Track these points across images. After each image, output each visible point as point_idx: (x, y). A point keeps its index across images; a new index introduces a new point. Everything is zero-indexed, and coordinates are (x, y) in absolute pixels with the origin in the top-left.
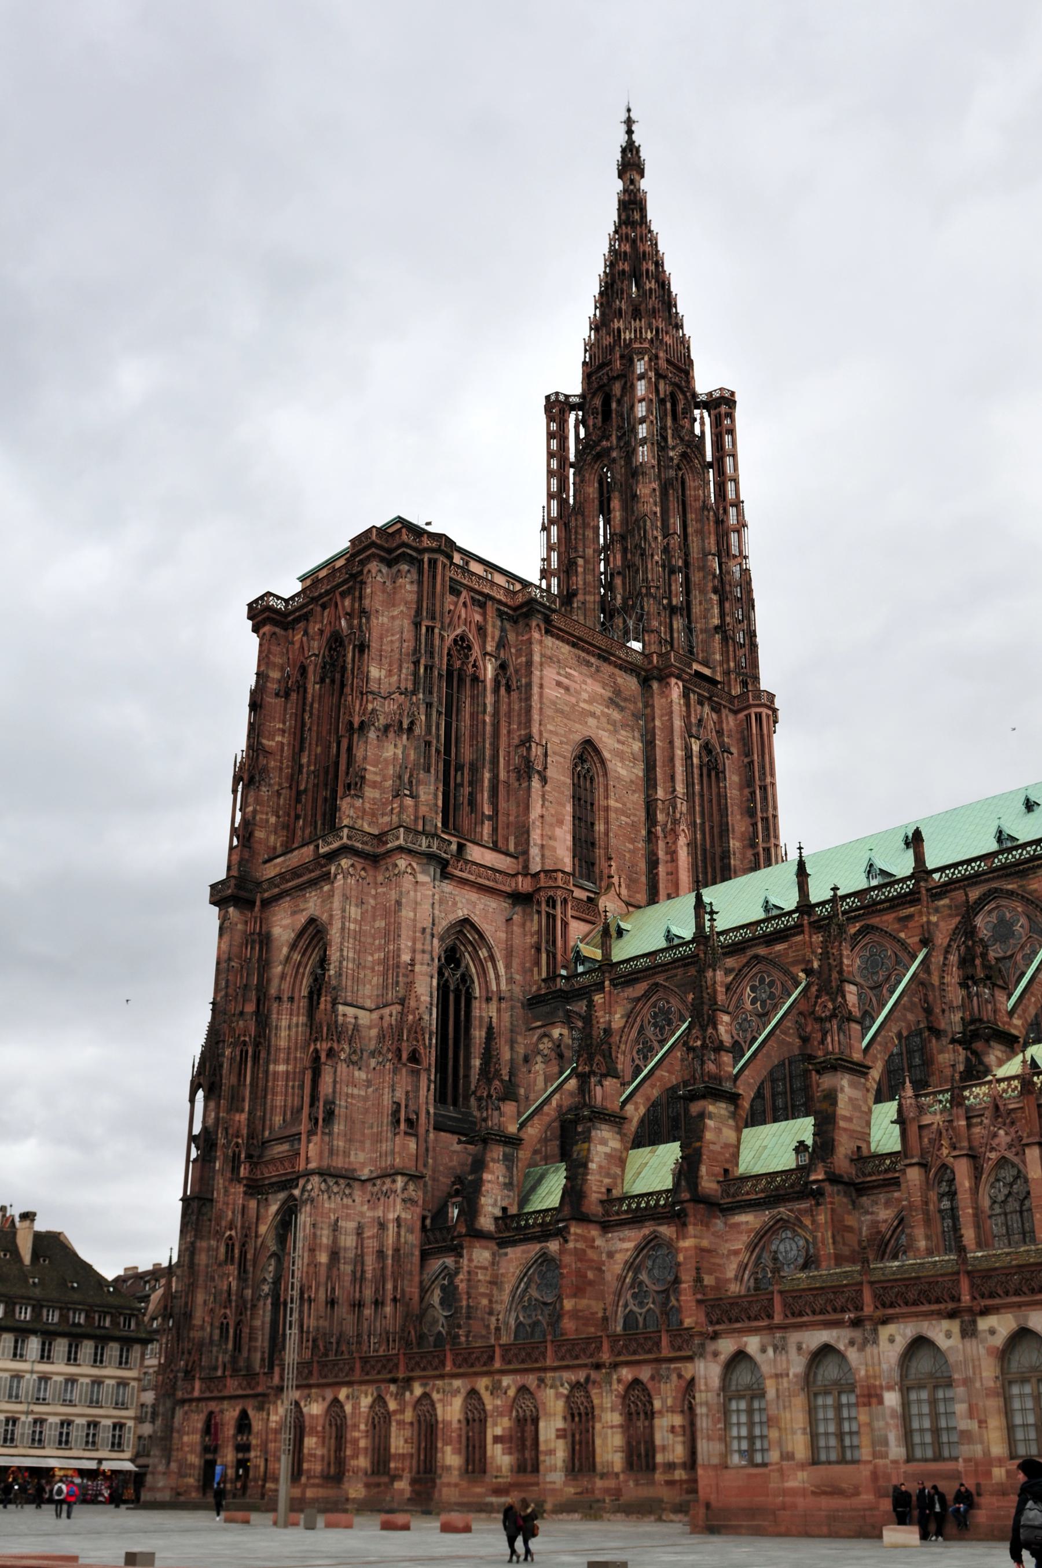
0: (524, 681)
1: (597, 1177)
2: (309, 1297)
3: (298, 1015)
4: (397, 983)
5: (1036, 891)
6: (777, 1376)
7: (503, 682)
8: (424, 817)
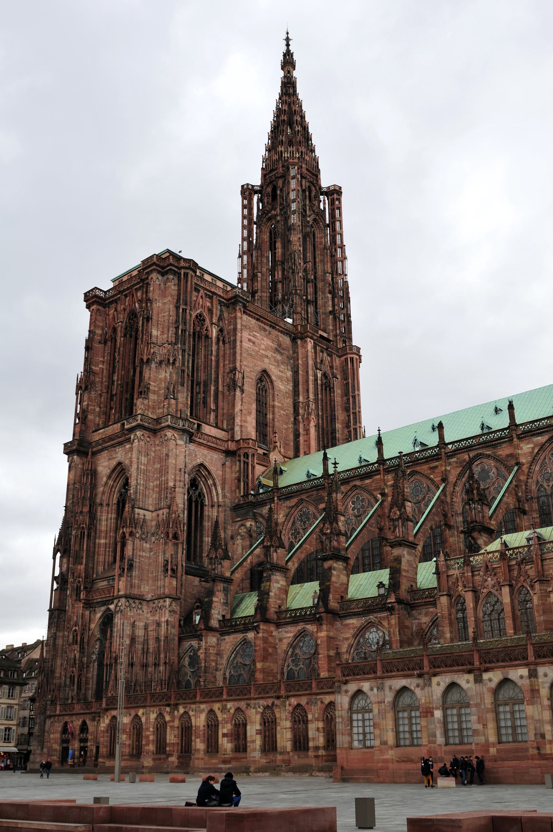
0: (232, 338)
1: (274, 600)
3: (112, 514)
4: (167, 497)
5: (501, 455)
6: (379, 703)
7: (221, 338)
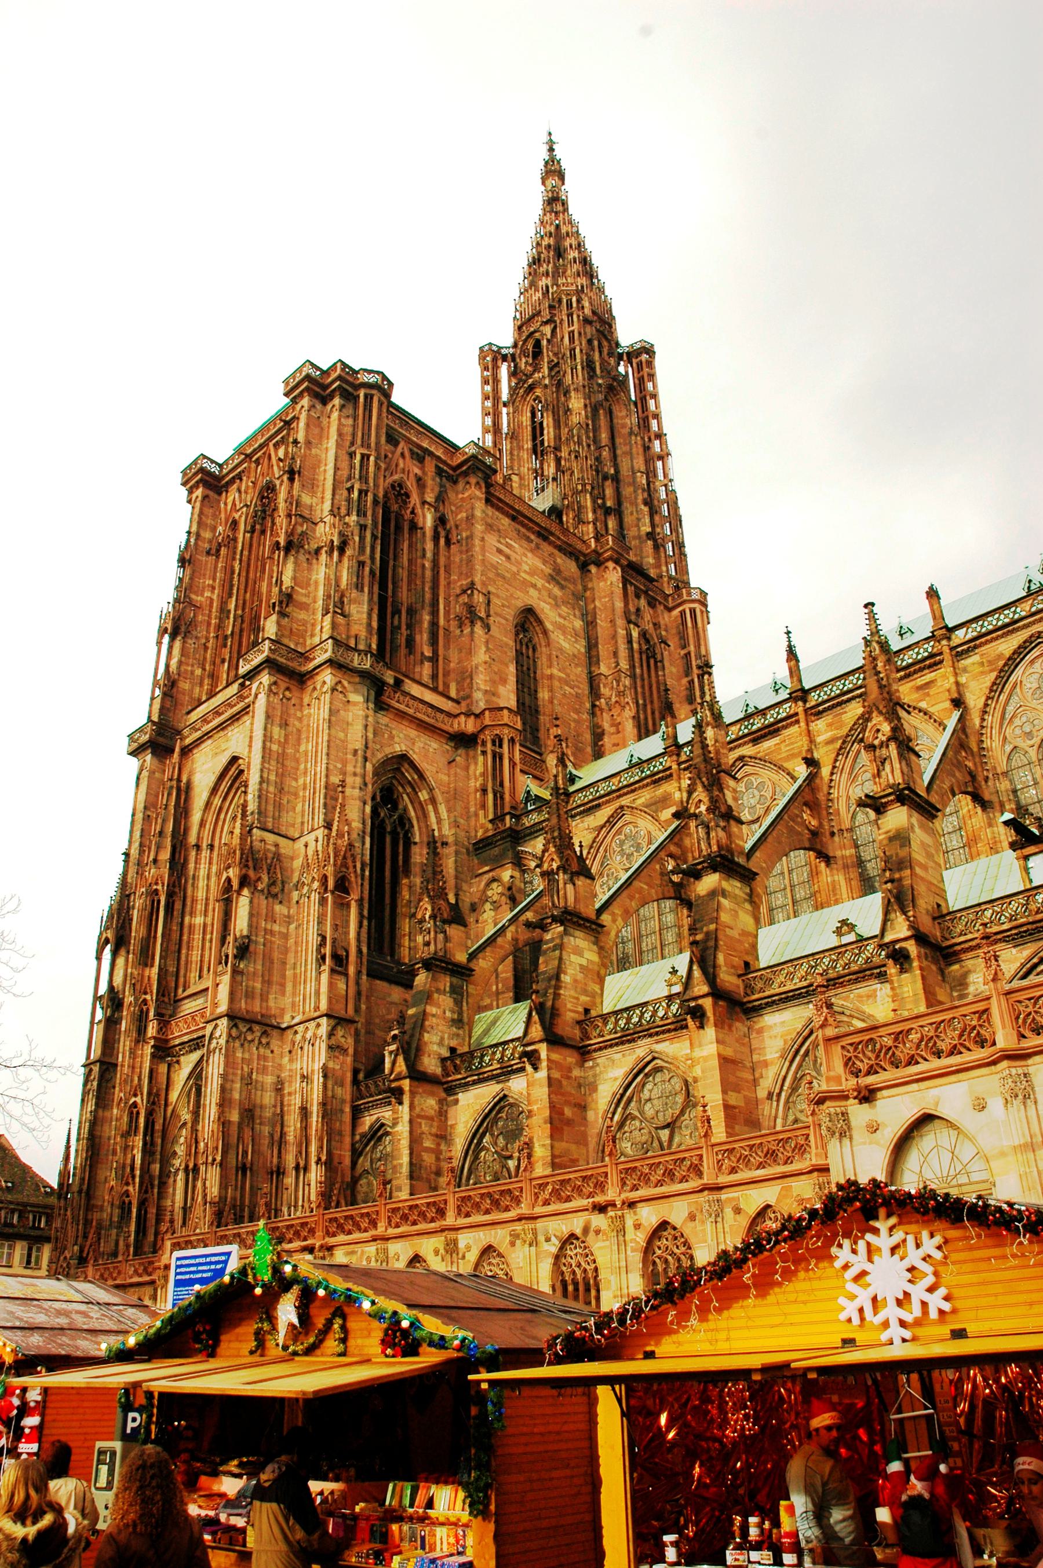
1: (572, 993)
2: (214, 1160)
7: (443, 534)
8: (356, 637)
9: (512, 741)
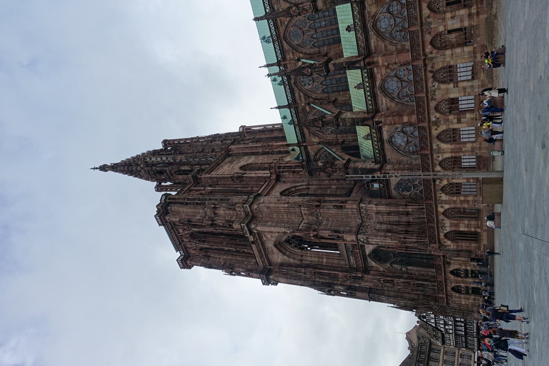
2: (403, 238)
3: (307, 253)
9: (280, 164)
